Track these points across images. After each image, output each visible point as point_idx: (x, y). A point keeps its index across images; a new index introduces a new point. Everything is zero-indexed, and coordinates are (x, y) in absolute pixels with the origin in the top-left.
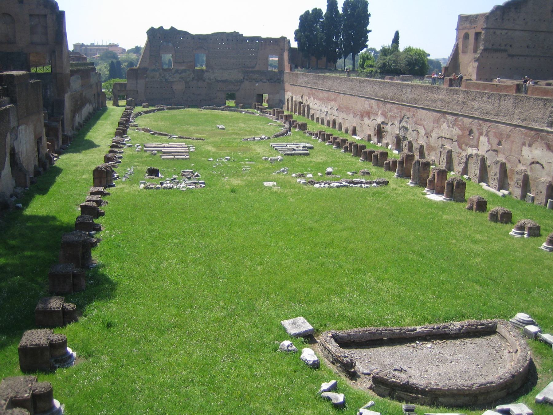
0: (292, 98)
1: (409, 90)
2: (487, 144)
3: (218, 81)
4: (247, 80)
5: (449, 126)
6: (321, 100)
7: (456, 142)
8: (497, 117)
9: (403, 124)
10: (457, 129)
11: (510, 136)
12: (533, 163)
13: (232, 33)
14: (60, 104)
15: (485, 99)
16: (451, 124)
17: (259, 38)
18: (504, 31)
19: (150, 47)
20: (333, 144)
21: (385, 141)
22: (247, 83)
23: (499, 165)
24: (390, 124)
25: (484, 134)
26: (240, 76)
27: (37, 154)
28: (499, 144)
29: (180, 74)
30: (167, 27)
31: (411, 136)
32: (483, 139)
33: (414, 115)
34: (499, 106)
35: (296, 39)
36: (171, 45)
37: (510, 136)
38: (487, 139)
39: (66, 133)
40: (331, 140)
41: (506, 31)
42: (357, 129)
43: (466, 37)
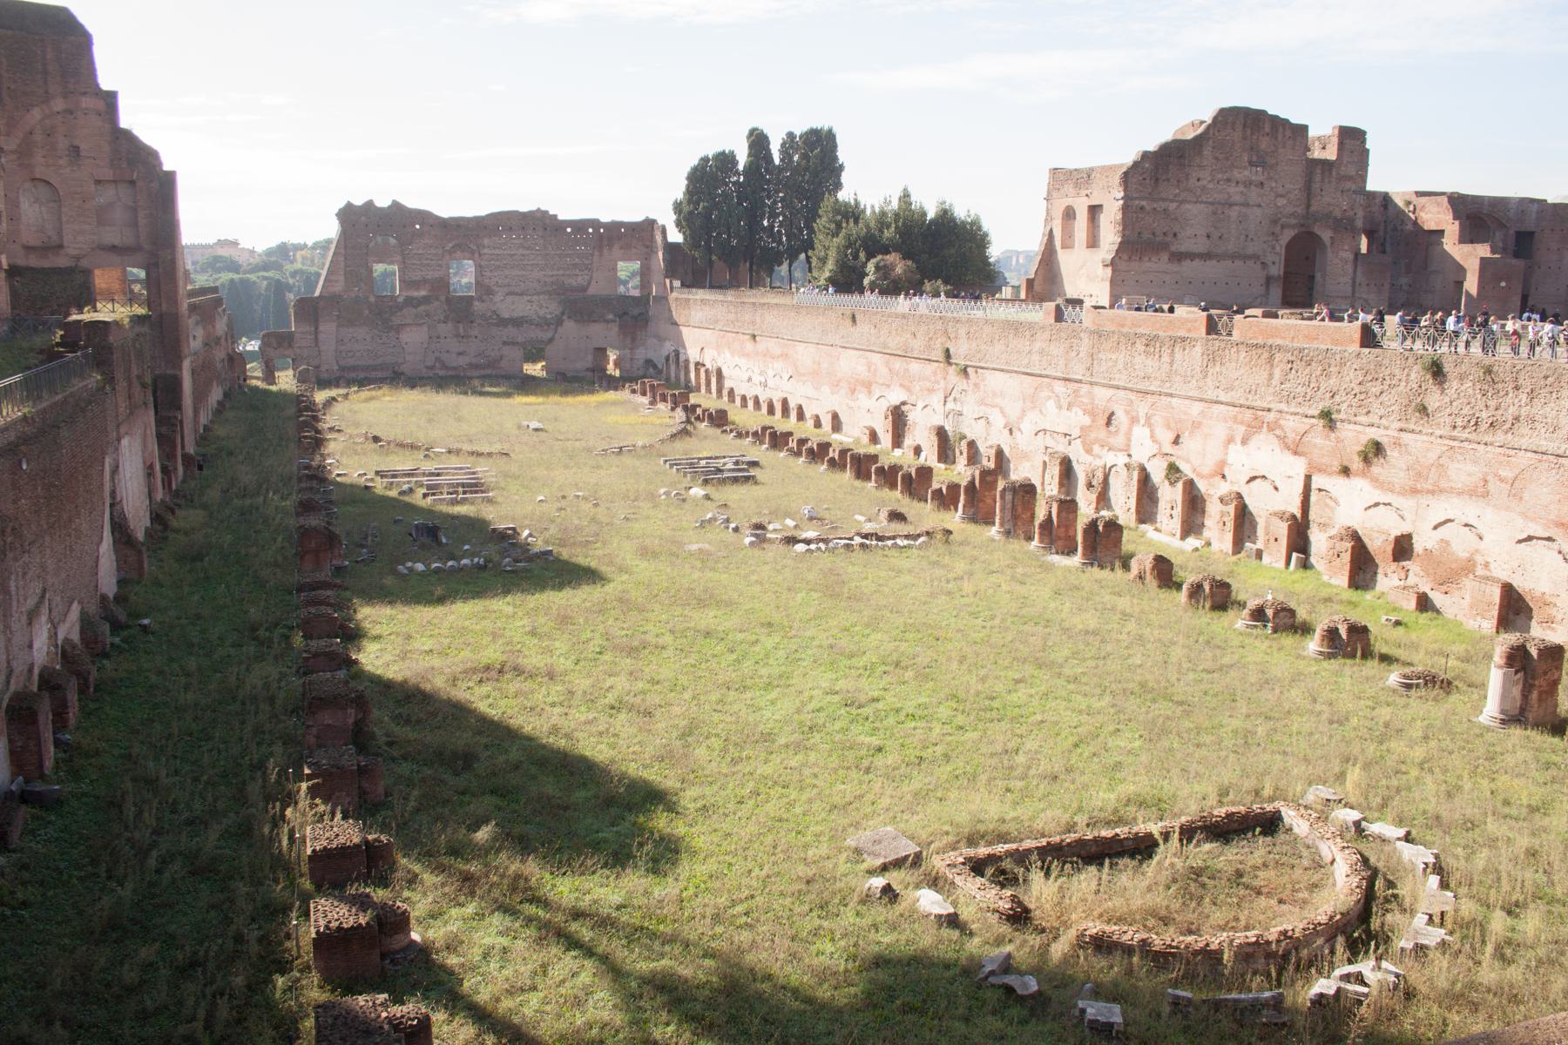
0: (677, 354)
1: (962, 332)
2: (1149, 442)
3: (503, 322)
5: (1060, 407)
6: (747, 355)
7: (1079, 441)
8: (1168, 385)
9: (950, 405)
10: (1080, 413)
11: (1200, 423)
12: (1253, 479)
13: (531, 213)
14: (174, 385)
15: (1140, 347)
16: (1065, 406)
17: (595, 223)
19: (346, 248)
20: (798, 454)
21: (909, 442)
23: (1180, 485)
24: (920, 405)
25: (1142, 421)
26: (551, 308)
28: (1176, 442)
29: (416, 307)
30: (383, 202)
31: (973, 430)
32: (1140, 433)
33: (976, 385)
34: (1171, 364)
35: (678, 224)
36: (392, 241)
37: (1200, 423)
38: (1147, 431)
39: (187, 450)
40: (793, 444)
42: (843, 417)
43: (1069, 214)
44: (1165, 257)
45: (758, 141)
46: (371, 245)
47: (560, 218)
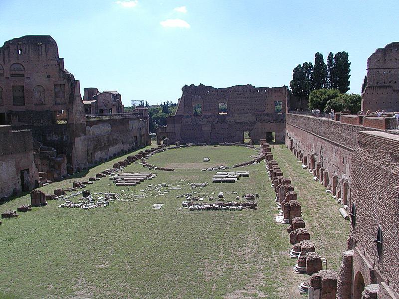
4: (259, 121)
14: (72, 144)
18: (387, 70)
22: (259, 124)
27: (20, 181)
30: (197, 84)
35: (292, 87)
36: (200, 97)
41: (390, 70)
44: (389, 90)
45: (319, 57)
46: (193, 98)
47: (256, 87)
